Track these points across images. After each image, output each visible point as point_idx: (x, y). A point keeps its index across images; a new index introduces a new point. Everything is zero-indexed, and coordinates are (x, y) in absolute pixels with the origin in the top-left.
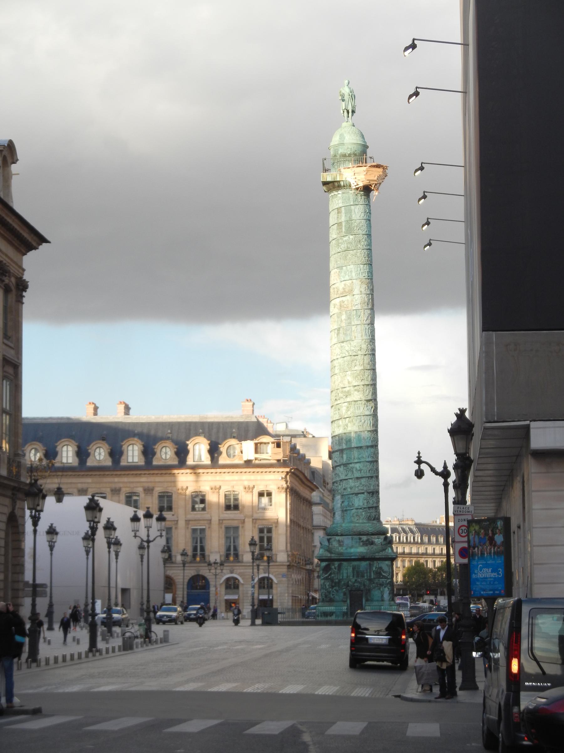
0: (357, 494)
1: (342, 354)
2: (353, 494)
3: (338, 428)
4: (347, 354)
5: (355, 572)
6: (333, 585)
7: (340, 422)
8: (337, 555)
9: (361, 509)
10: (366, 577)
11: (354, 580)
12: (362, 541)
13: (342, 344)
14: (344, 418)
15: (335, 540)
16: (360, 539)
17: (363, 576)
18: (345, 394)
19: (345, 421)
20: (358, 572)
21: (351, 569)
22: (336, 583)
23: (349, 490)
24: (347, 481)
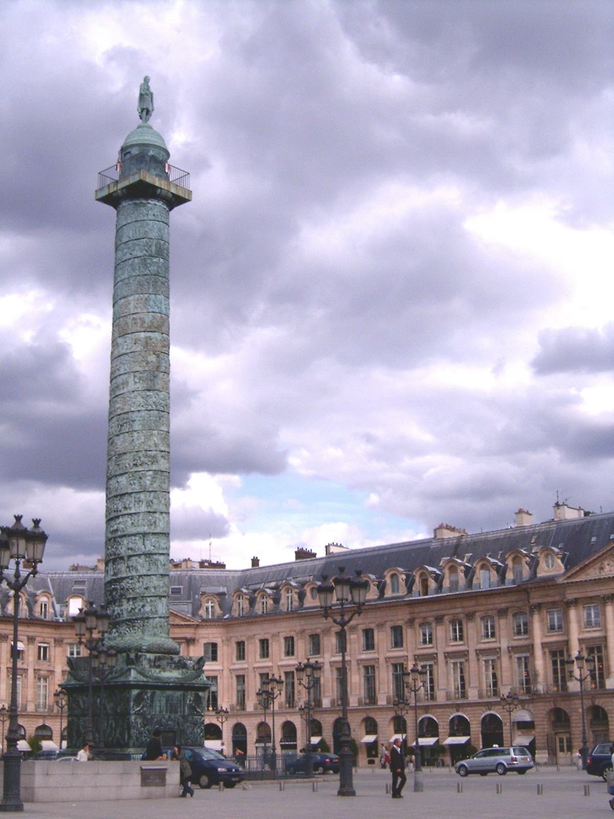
0: (161, 597)
1: (147, 406)
2: (156, 596)
3: (138, 504)
4: (154, 406)
5: (169, 705)
6: (145, 723)
7: (142, 496)
8: (154, 681)
9: (164, 617)
10: (179, 713)
11: (167, 717)
12: (175, 663)
13: (148, 393)
14: (148, 492)
15: (146, 658)
16: (172, 659)
17: (176, 712)
18: (150, 459)
19: (150, 496)
20: (171, 706)
21: (164, 702)
22: (148, 719)
23: (153, 590)
24: (149, 577)
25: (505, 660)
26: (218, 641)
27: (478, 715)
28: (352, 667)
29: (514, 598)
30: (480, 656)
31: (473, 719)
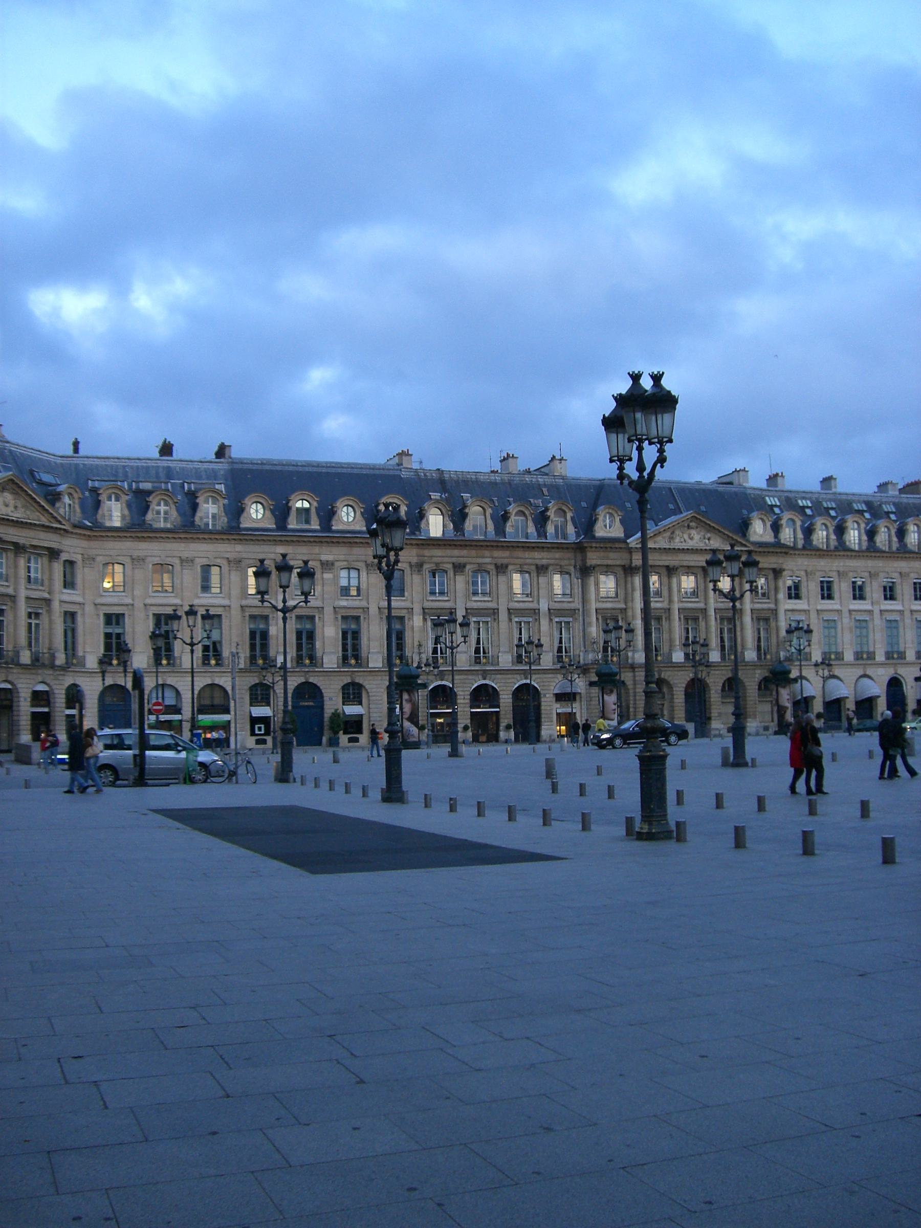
25: (544, 623)
26: (78, 558)
27: (510, 685)
28: (326, 617)
29: (557, 555)
30: (513, 616)
31: (505, 688)
